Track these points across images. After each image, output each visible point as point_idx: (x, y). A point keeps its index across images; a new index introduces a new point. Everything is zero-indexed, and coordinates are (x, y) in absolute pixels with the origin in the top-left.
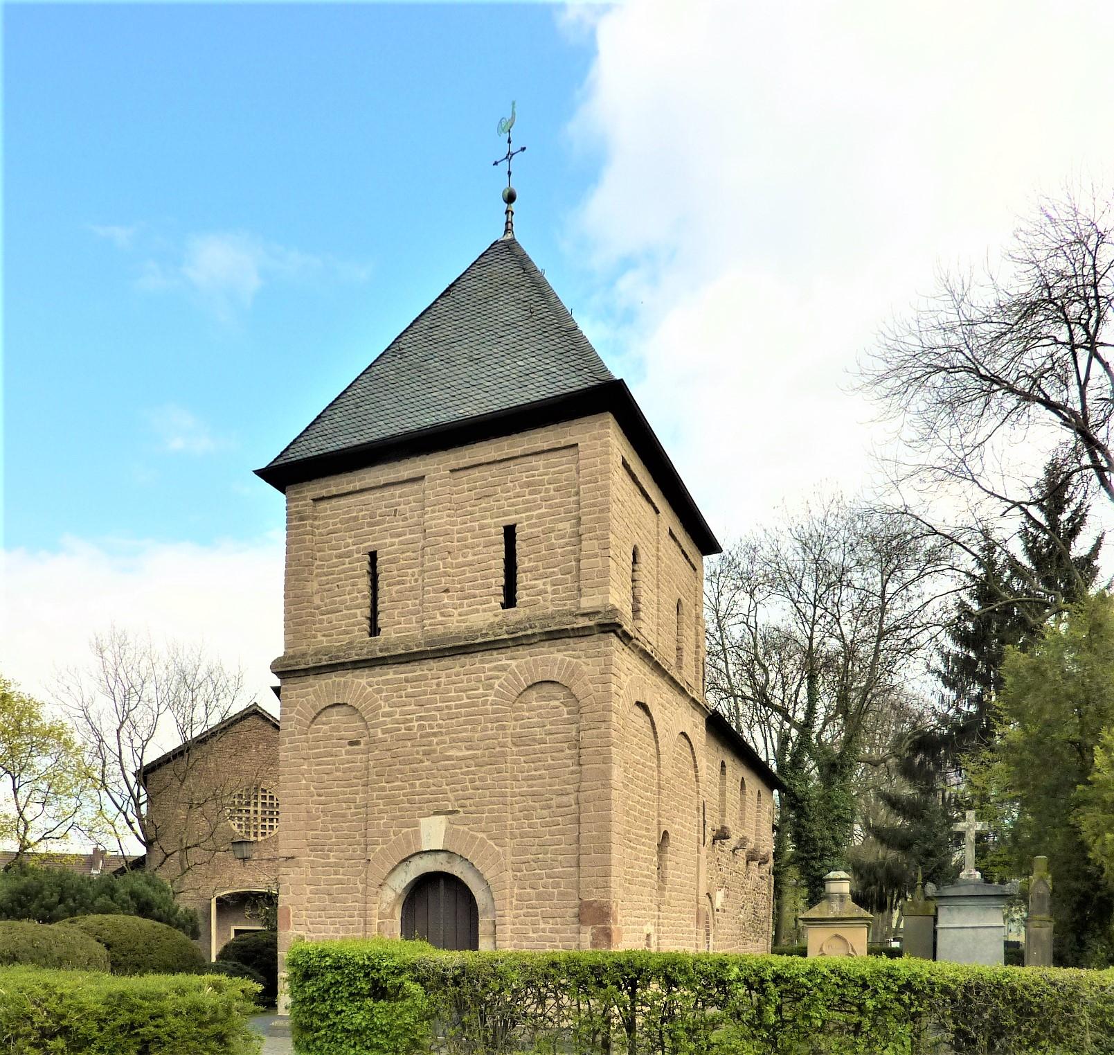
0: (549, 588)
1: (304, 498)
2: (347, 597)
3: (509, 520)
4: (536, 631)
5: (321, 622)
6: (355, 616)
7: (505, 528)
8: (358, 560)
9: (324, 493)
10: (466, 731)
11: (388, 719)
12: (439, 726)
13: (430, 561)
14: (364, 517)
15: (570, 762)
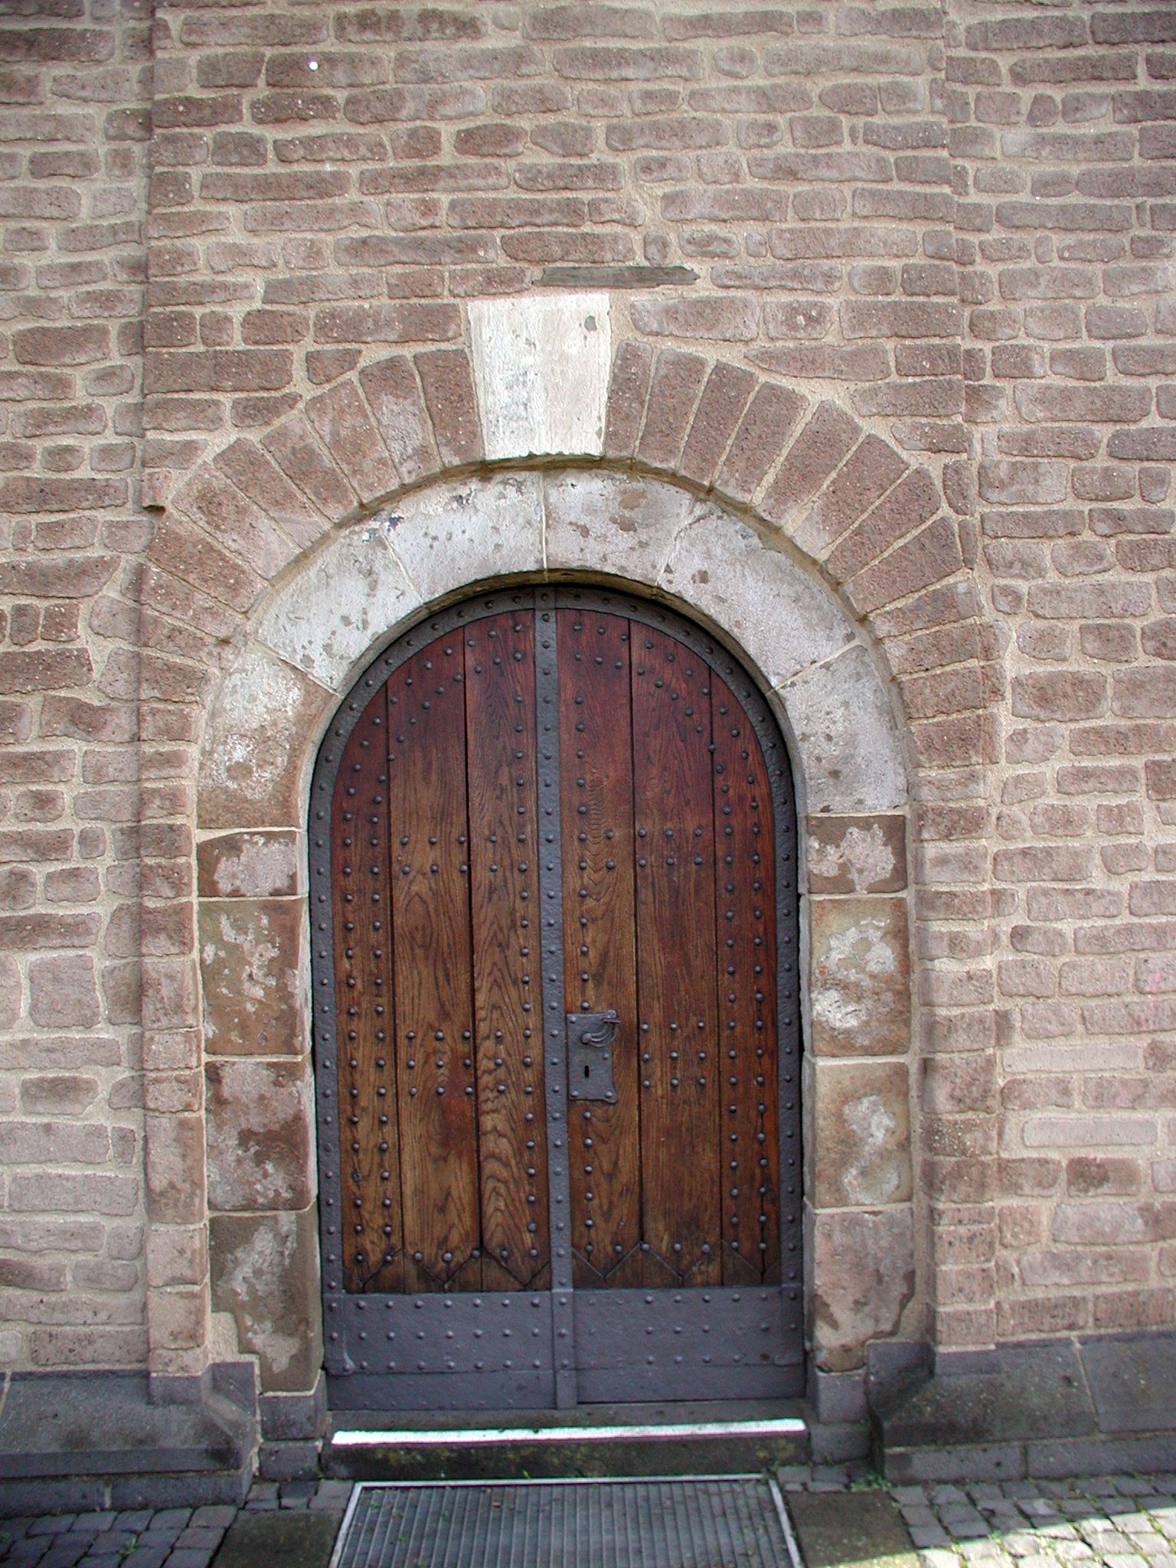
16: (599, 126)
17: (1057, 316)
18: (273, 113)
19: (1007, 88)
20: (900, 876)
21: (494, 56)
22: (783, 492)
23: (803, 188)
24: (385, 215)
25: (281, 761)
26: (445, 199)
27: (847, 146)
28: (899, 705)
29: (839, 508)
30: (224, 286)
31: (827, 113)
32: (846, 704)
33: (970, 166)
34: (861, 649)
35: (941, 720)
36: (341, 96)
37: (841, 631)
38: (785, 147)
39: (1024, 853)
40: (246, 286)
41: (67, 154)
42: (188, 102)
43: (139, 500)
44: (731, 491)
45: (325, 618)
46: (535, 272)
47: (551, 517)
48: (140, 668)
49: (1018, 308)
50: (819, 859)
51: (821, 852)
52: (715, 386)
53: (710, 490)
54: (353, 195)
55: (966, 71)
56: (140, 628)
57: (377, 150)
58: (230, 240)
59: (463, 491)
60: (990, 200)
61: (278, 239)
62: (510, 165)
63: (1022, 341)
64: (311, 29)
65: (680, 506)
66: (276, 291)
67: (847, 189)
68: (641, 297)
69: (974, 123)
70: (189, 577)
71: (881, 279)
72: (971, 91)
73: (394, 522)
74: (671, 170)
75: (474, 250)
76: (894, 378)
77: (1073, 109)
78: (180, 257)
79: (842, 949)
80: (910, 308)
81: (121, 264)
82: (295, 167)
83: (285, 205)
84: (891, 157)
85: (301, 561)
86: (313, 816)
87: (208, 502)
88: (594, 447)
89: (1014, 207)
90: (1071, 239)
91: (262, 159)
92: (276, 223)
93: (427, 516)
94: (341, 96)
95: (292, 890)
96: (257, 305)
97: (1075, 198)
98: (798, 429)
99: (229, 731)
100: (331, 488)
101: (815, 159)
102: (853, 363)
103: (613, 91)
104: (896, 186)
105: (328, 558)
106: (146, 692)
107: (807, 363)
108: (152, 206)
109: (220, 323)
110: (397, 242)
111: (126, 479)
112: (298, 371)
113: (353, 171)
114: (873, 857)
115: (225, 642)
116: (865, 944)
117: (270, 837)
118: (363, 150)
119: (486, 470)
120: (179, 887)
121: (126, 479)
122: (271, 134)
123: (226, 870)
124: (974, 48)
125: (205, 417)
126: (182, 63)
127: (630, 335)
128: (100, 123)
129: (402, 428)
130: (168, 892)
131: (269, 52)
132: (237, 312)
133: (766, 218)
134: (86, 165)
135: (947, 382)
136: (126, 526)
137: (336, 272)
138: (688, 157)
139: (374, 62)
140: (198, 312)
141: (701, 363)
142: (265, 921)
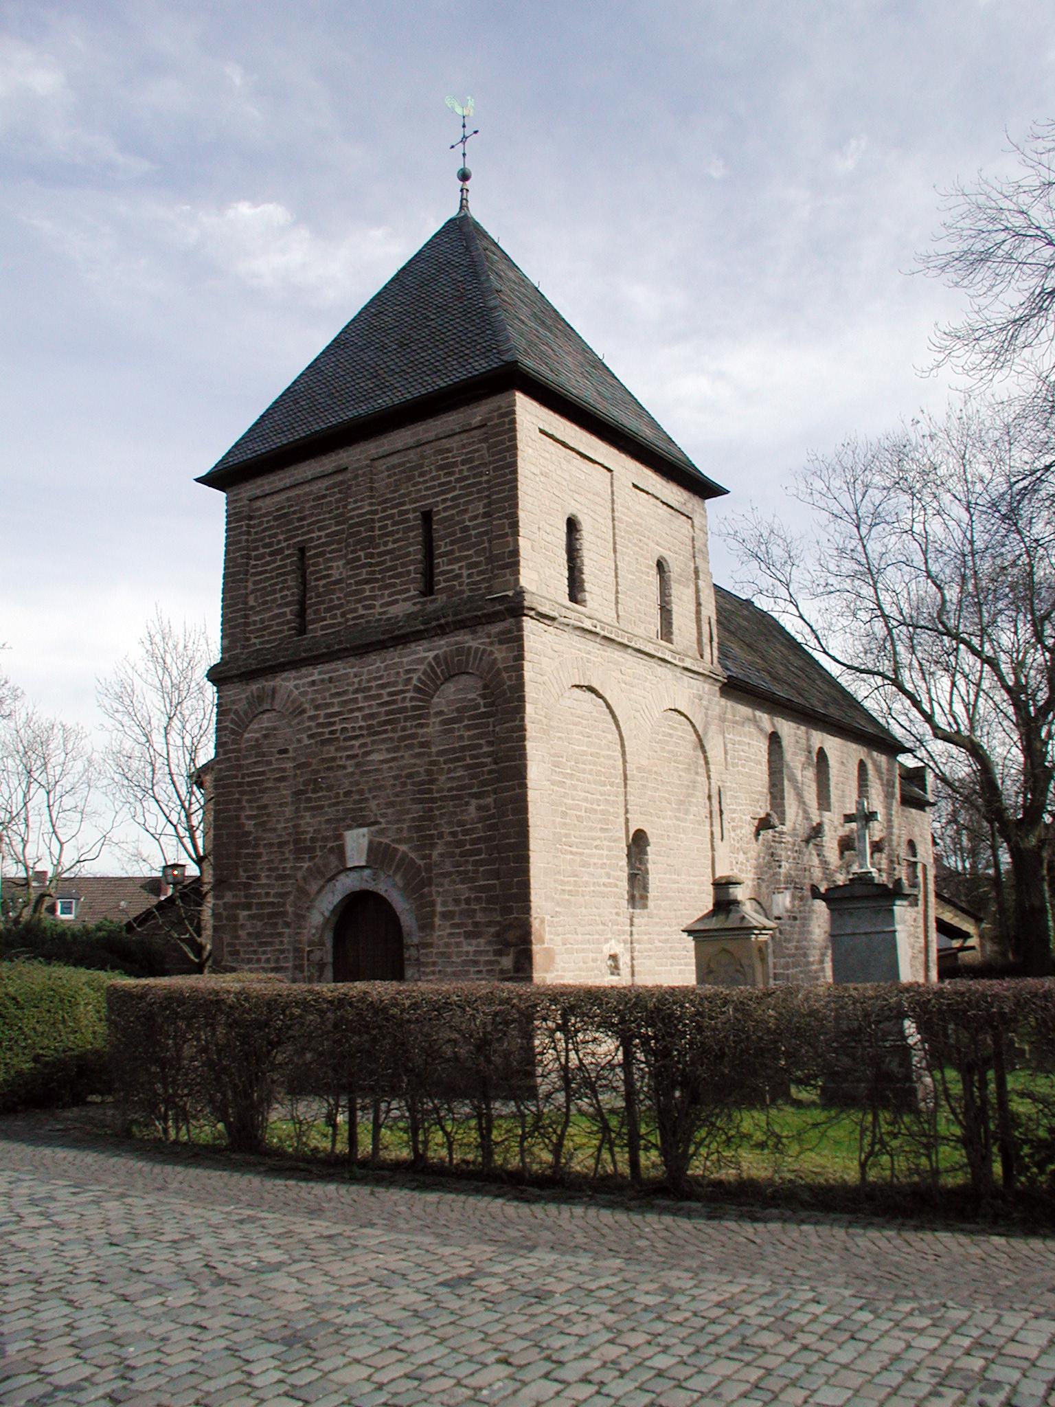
1: (241, 499)
5: (255, 623)
6: (284, 614)
9: (258, 492)
17: (450, 823)
35: (426, 925)
45: (328, 901)
68: (373, 828)
71: (413, 819)
87: (304, 879)
88: (363, 864)
102: (408, 840)
107: (399, 841)
129: (333, 861)
135: (425, 842)
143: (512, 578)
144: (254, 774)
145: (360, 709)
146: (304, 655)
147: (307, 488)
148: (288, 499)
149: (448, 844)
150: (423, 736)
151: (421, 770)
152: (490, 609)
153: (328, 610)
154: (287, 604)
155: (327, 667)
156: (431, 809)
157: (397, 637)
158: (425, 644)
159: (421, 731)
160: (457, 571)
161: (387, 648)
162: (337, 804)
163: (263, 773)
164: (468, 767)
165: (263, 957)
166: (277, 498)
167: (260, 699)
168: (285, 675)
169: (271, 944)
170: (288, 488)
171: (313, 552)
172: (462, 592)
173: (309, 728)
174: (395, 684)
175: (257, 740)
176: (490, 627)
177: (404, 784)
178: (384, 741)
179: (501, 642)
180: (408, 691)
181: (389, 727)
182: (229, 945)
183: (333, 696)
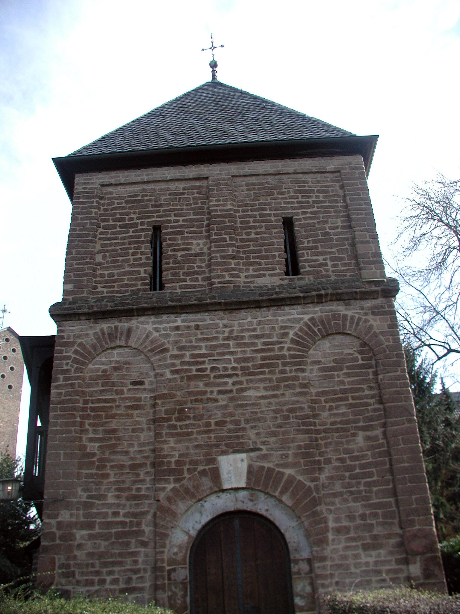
0: (330, 263)
2: (131, 258)
3: (288, 212)
4: (329, 292)
5: (102, 276)
6: (139, 272)
7: (284, 218)
8: (142, 230)
9: (113, 181)
10: (263, 373)
11: (177, 362)
12: (234, 368)
13: (215, 234)
14: (149, 200)
15: (372, 401)
16: (242, 419)
17: (336, 451)
18: (179, 419)
19: (324, 404)
20: (311, 571)
21: (221, 406)
22: (282, 493)
23: (283, 429)
24: (201, 439)
25: (184, 551)
26: (213, 436)
27: (292, 420)
28: (308, 536)
29: (293, 495)
30: (170, 455)
31: (287, 413)
32: (297, 535)
33: (317, 421)
34: (300, 523)
36: (192, 415)
37: (295, 520)
38: (279, 421)
39: (336, 565)
40: (175, 455)
41: (138, 428)
42: (163, 418)
43: (155, 498)
44: (272, 493)
45: (192, 521)
46: (231, 450)
47: (237, 500)
48: (156, 533)
49: (328, 450)
50: (294, 568)
51: (294, 566)
52: (267, 472)
53: (268, 493)
54: (195, 436)
55: (314, 401)
56: (155, 525)
57: (199, 426)
58: (171, 445)
59: (219, 495)
60: (322, 428)
61: (181, 445)
62: (225, 428)
63: (330, 456)
64: (185, 403)
65: (262, 496)
66: (181, 455)
67: (292, 429)
68: (252, 454)
69: (317, 412)
70: (165, 514)
71: (300, 447)
72: (316, 405)
73: (205, 501)
74: (257, 428)
75: (219, 446)
76: (303, 467)
77: (337, 407)
78: (162, 449)
79: (300, 586)
80: (306, 452)
81: (150, 450)
82: (184, 430)
83: (182, 438)
84: (300, 421)
85: (187, 511)
86: (190, 563)
87: (169, 499)
89: (326, 429)
90: (338, 434)
91: (177, 429)
92: (180, 442)
93: (212, 500)
94: (192, 415)
95: (186, 579)
96: (177, 459)
97: (339, 426)
98: (284, 479)
99: (173, 545)
100: (193, 496)
101: (285, 423)
103: (245, 412)
104: (302, 427)
105: (193, 509)
106: (157, 538)
107: (286, 466)
108: (155, 439)
109: (170, 462)
110: (204, 445)
111: (152, 494)
112: (186, 472)
113: (195, 431)
114: (305, 567)
115: (172, 527)
116: (304, 586)
117: (182, 568)
118: (197, 427)
119: (223, 491)
120: (164, 579)
121: (152, 494)
122: (179, 424)
123: (173, 575)
124: (316, 396)
125: (167, 481)
126: (161, 410)
127: (251, 462)
128: (145, 421)
129: (206, 482)
130: (162, 580)
131: (178, 407)
132: (173, 460)
133: (276, 436)
134: (142, 430)
135: (314, 467)
136: (152, 504)
137: (192, 451)
138: (260, 424)
139: (198, 408)
140: (165, 460)
141: (264, 467)
142: (181, 586)
143: (378, 271)
144: (99, 401)
145: (232, 353)
146: (170, 303)
147: (163, 186)
148: (143, 190)
149: (336, 468)
150: (303, 379)
151: (305, 406)
152: (367, 288)
153: (188, 274)
154: (141, 265)
155: (191, 317)
156: (316, 440)
157: (275, 301)
158: (299, 308)
159: (301, 375)
160: (321, 262)
161: (260, 307)
162: (209, 431)
163: (114, 400)
164: (351, 406)
165: (109, 579)
166: (129, 188)
167: (112, 336)
168: (142, 319)
169: (120, 563)
170: (144, 183)
171: (170, 230)
172: (328, 276)
173: (173, 365)
174: (269, 336)
175: (105, 371)
176: (362, 302)
177: (288, 417)
178: (261, 380)
179: (374, 313)
180: (286, 342)
181: (267, 370)
182: (62, 566)
183: (200, 340)
